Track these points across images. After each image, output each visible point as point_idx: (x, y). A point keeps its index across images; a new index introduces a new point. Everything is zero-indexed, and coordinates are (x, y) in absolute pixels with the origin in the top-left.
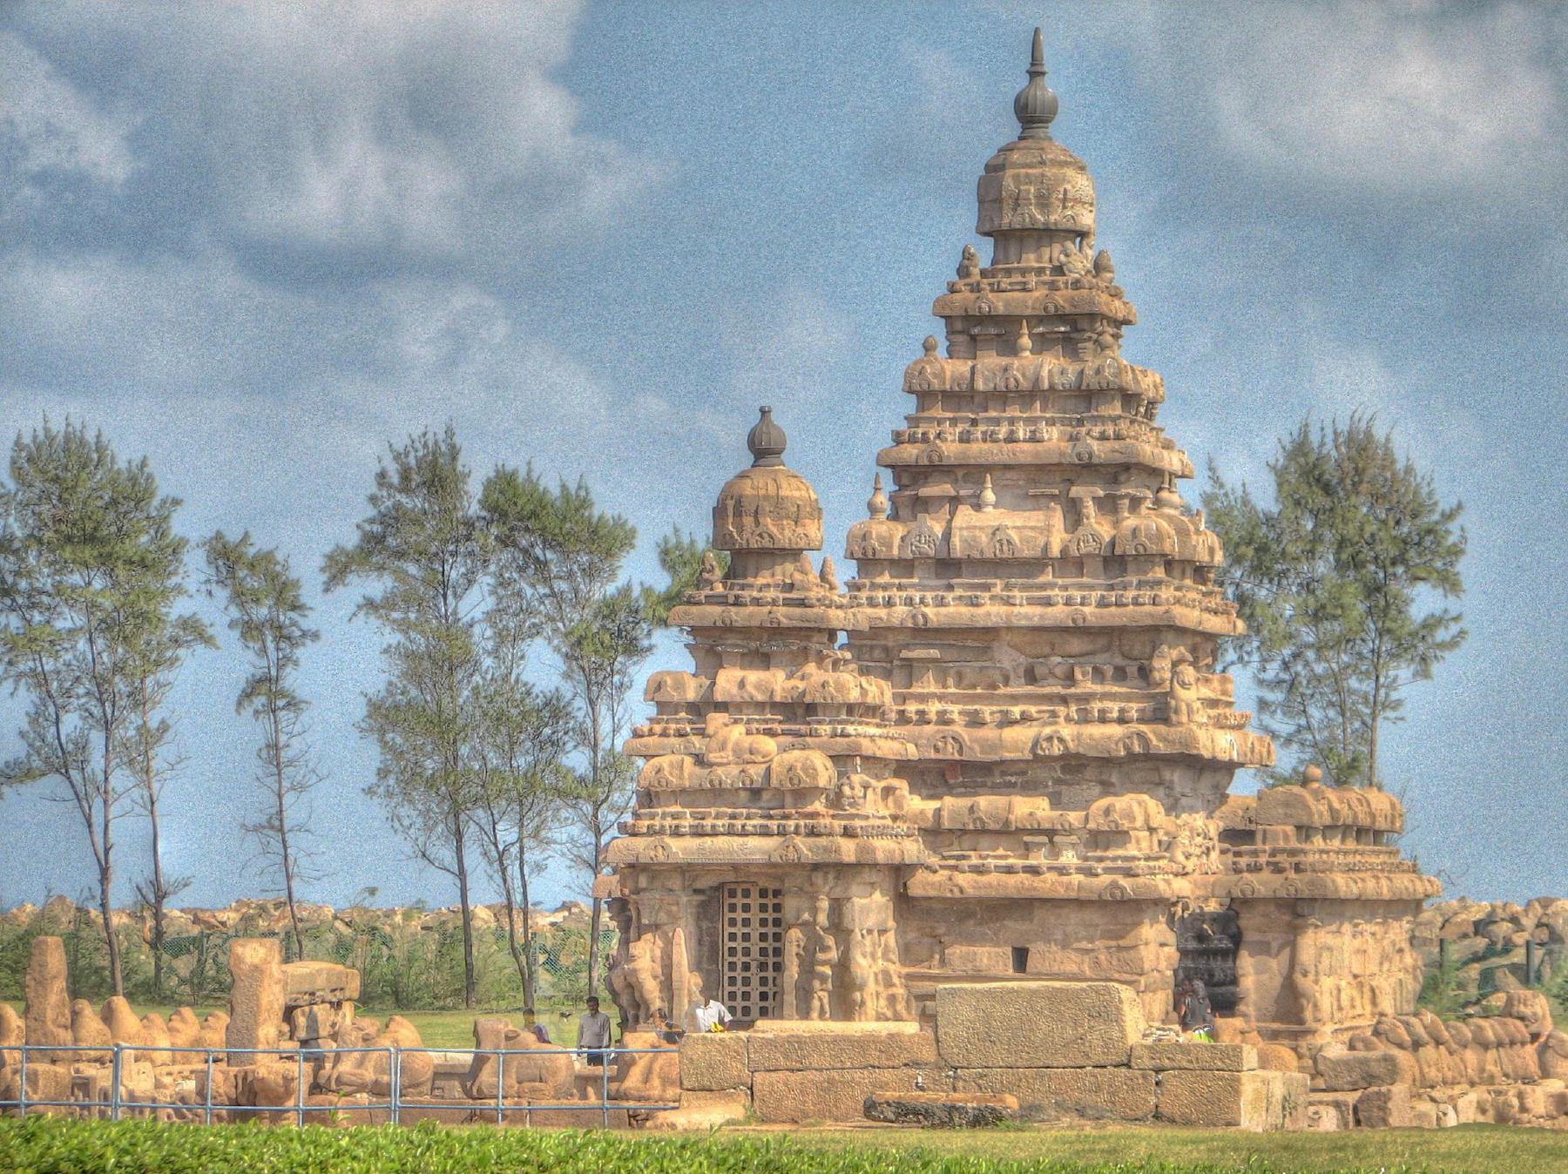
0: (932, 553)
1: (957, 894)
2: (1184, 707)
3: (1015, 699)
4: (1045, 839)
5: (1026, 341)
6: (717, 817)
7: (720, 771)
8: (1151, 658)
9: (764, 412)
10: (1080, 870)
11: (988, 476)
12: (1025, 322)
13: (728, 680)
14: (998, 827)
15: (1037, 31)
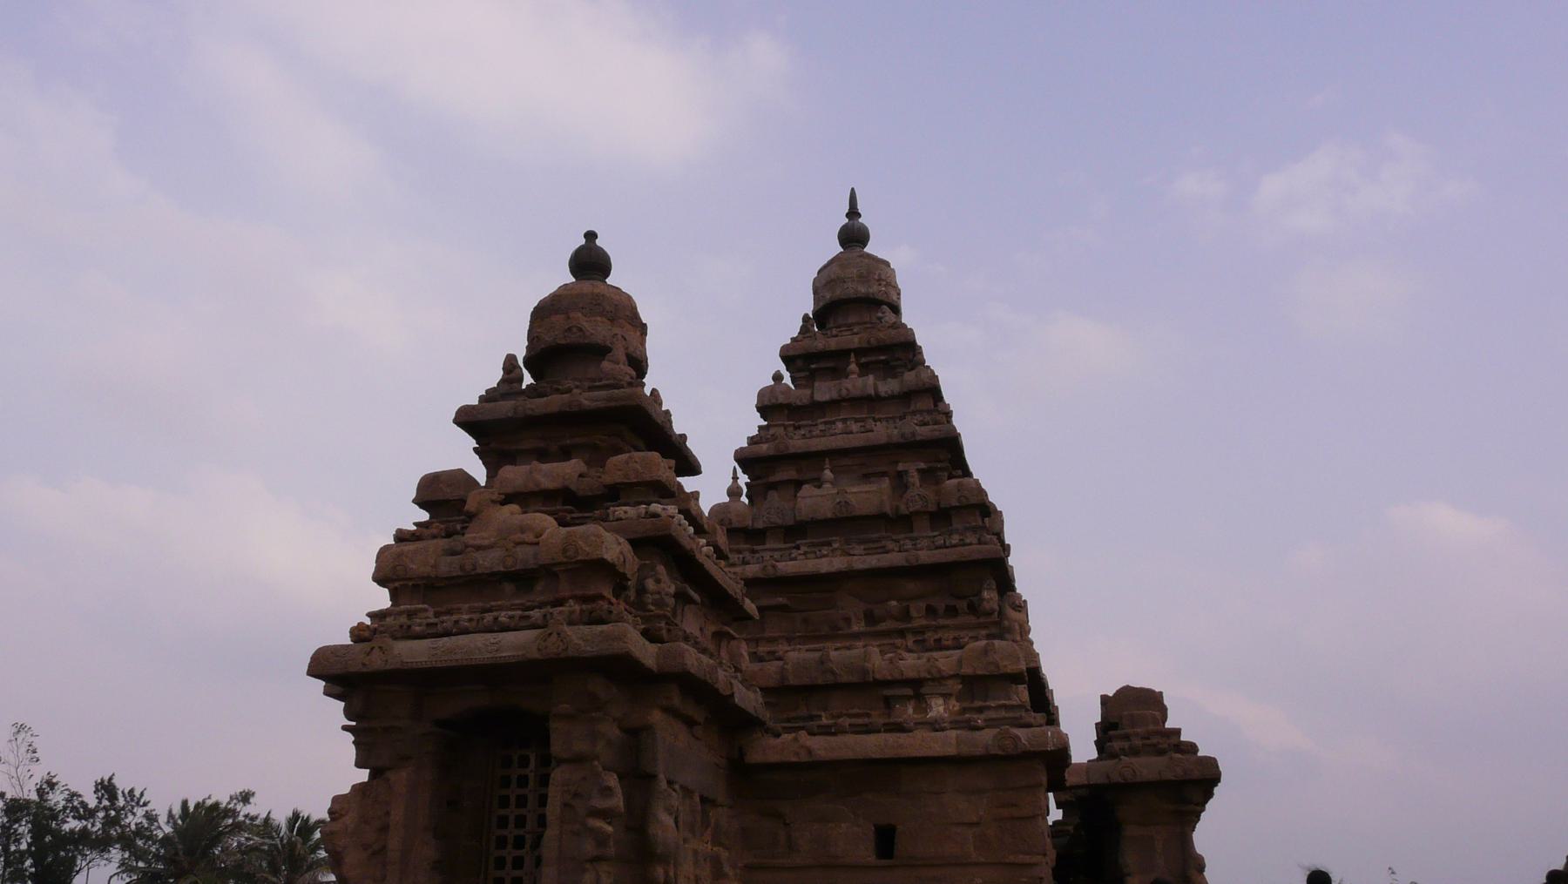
0: (779, 522)
1: (804, 758)
2: (1017, 627)
3: (857, 636)
4: (909, 691)
5: (853, 367)
6: (471, 611)
7: (478, 555)
8: (979, 593)
9: (591, 236)
10: (956, 725)
11: (827, 460)
12: (852, 355)
13: (514, 475)
14: (854, 679)
15: (853, 189)
